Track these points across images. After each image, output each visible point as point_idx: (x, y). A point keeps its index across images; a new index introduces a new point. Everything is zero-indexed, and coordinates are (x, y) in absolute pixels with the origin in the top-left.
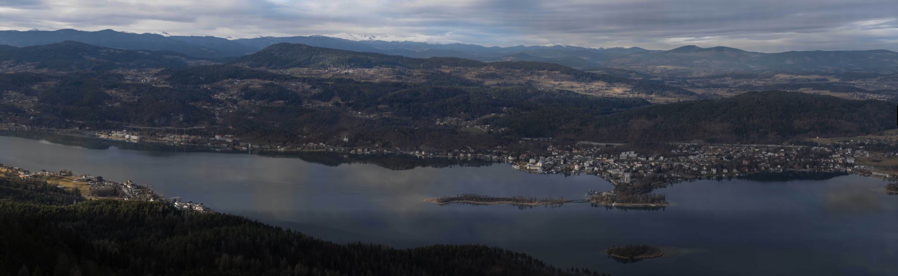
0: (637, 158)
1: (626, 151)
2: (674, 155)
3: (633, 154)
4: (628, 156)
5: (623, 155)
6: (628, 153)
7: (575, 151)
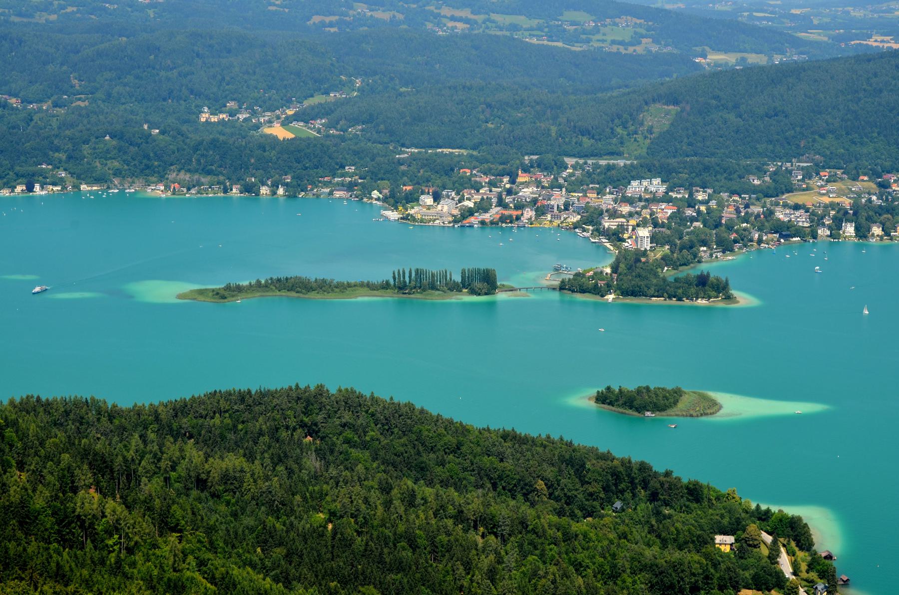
0: (667, 193)
1: (640, 178)
2: (754, 190)
3: (657, 186)
4: (646, 189)
5: (635, 188)
6: (645, 183)
7: (522, 178)
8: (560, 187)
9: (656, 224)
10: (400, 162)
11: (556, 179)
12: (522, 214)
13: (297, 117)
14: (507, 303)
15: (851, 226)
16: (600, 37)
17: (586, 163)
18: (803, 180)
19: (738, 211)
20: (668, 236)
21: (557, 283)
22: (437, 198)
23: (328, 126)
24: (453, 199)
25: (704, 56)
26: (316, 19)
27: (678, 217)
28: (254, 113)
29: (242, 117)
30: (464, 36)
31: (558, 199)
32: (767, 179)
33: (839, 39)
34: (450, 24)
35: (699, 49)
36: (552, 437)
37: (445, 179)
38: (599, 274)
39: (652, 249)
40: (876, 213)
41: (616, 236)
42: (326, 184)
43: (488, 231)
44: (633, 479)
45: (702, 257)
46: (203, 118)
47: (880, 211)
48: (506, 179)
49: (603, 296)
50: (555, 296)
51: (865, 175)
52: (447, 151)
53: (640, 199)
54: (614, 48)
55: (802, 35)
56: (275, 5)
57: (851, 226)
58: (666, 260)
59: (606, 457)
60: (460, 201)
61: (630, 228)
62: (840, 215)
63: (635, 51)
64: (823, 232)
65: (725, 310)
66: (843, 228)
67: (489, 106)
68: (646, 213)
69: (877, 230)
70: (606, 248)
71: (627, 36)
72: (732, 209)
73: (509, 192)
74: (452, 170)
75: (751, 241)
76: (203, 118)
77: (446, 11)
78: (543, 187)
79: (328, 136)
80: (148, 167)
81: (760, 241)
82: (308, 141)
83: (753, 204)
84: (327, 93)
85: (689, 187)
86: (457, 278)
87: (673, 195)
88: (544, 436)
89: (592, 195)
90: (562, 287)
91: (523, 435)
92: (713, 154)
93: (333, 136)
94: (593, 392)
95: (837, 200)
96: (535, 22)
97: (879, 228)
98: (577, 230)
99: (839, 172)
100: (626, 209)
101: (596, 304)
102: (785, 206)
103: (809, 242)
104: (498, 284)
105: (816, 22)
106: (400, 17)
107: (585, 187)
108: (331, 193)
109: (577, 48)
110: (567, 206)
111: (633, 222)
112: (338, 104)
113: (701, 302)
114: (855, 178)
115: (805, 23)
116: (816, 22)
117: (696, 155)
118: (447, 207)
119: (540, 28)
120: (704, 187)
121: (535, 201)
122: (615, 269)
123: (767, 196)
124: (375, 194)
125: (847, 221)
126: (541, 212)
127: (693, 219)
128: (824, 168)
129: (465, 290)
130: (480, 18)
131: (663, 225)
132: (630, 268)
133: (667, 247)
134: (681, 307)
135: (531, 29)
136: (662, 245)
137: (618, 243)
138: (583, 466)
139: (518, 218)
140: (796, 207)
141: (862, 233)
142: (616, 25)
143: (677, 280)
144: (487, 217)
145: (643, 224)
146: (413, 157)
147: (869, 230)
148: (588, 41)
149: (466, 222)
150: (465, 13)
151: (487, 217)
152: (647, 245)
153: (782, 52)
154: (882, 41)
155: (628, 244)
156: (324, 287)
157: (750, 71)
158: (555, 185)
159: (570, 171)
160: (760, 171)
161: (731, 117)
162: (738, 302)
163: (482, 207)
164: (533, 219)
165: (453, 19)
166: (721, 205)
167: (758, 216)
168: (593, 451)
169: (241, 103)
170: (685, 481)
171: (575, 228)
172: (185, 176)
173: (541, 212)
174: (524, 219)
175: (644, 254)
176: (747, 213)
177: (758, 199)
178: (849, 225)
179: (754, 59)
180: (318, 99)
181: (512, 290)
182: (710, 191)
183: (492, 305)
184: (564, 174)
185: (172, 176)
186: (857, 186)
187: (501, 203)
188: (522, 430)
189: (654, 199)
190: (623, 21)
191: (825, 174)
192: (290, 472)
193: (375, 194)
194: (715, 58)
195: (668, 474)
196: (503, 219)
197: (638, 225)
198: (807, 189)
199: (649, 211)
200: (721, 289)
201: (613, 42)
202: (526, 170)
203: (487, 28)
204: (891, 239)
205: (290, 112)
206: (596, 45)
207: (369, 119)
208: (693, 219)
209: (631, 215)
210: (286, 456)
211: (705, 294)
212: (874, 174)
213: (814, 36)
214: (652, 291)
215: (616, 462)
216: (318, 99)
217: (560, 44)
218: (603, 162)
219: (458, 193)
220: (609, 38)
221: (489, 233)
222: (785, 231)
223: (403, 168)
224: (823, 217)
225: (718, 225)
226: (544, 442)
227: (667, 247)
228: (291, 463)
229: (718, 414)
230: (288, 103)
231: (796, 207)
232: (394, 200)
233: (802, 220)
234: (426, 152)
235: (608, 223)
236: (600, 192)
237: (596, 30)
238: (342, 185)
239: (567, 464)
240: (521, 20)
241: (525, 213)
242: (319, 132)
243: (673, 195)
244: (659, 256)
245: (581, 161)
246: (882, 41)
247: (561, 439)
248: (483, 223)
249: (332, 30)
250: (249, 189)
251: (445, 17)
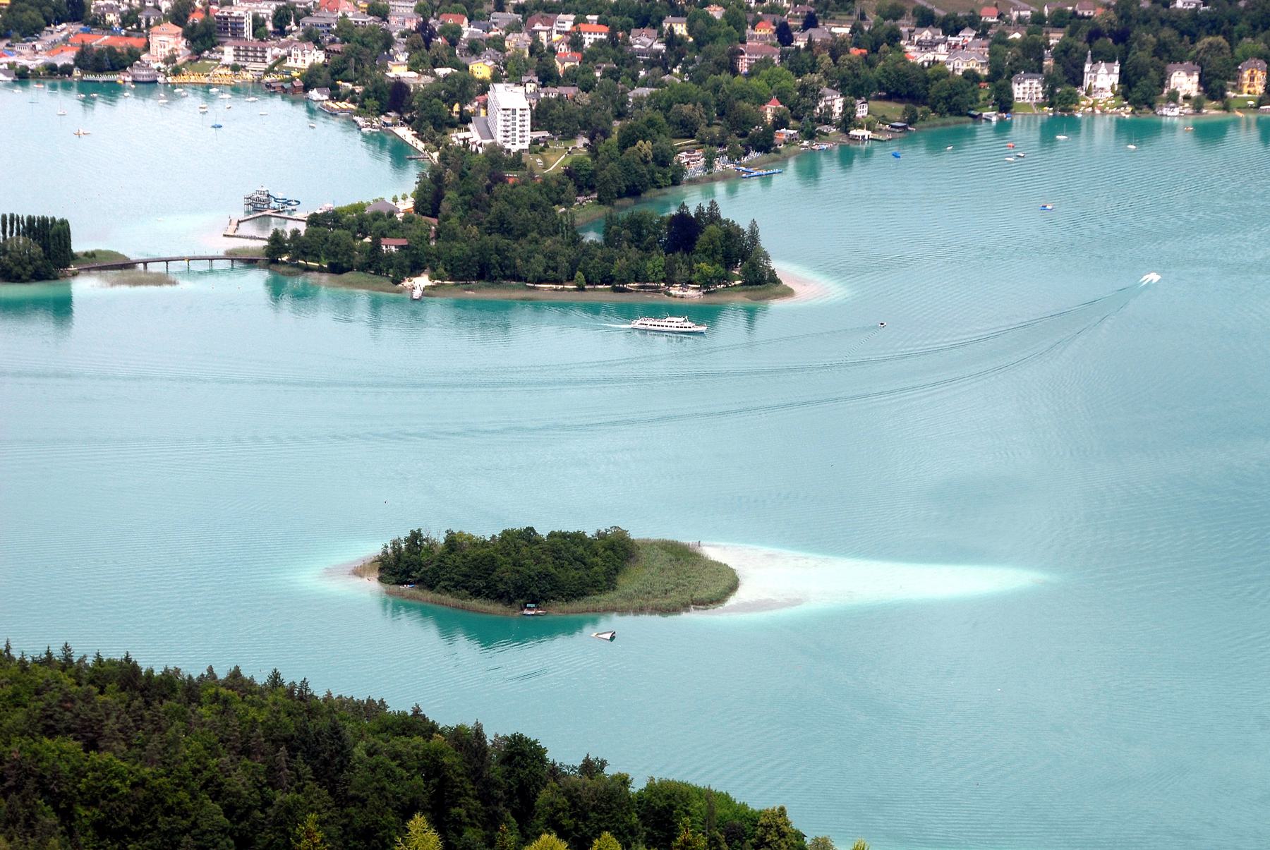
15: (1110, 72)
19: (784, 35)
20: (586, 110)
21: (258, 244)
36: (246, 674)
40: (1182, 33)
43: (39, 93)
44: (490, 784)
45: (681, 170)
57: (1110, 72)
58: (580, 179)
59: (415, 724)
64: (1026, 90)
66: (1087, 81)
69: (1184, 82)
72: (766, 31)
81: (848, 121)
88: (222, 674)
91: (158, 672)
94: (374, 548)
97: (1189, 74)
98: (314, 94)
103: (989, 121)
104: (78, 247)
125: (1098, 57)
133: (581, 141)
136: (570, 136)
138: (343, 752)
139: (132, 57)
147: (1163, 80)
162: (788, 293)
164: (180, 60)
168: (372, 709)
170: (638, 785)
171: (306, 88)
174: (153, 59)
175: (517, 162)
178: (1103, 68)
188: (152, 661)
195: (590, 768)
199: (526, 36)
204: (1226, 108)
211: (692, 271)
215: (437, 740)
226: (223, 690)
227: (581, 141)
229: (732, 601)
239: (293, 751)
241: (155, 41)
247: (275, 679)
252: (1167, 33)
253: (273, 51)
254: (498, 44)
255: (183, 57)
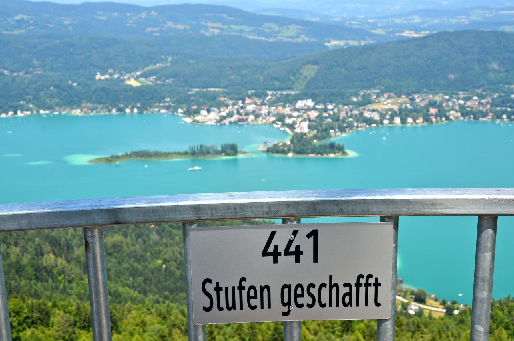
0: (314, 106)
1: (302, 99)
2: (354, 103)
3: (310, 103)
4: (305, 105)
5: (300, 104)
6: (304, 101)
7: (248, 101)
8: (265, 105)
9: (310, 120)
10: (191, 95)
11: (263, 101)
12: (248, 118)
13: (142, 76)
14: (242, 159)
16: (281, 34)
17: (277, 93)
18: (376, 98)
19: (347, 113)
21: (265, 149)
22: (209, 111)
23: (157, 79)
24: (216, 112)
25: (329, 42)
26: (149, 29)
27: (320, 117)
28: (121, 75)
29: (116, 76)
30: (219, 36)
31: (265, 110)
32: (360, 98)
33: (390, 33)
34: (212, 30)
35: (327, 39)
37: (212, 102)
38: (284, 145)
39: (309, 132)
41: (292, 127)
42: (157, 107)
46: (98, 77)
47: (411, 111)
48: (240, 102)
49: (287, 154)
50: (265, 155)
51: (404, 94)
52: (212, 89)
53: (302, 109)
54: (288, 40)
55: (374, 31)
56: (128, 23)
58: (315, 137)
60: (220, 112)
61: (298, 123)
62: (393, 114)
63: (298, 41)
64: (386, 122)
65: (343, 159)
67: (231, 68)
68: (305, 116)
69: (410, 120)
70: (287, 133)
71: (294, 34)
72: (344, 113)
73: (242, 108)
74: (215, 98)
75: (353, 126)
76: (98, 77)
77: (210, 24)
78: (258, 105)
79: (157, 84)
80: (72, 101)
81: (357, 127)
82: (148, 87)
83: (354, 110)
84: (155, 64)
85: (325, 103)
86: (219, 148)
87: (317, 107)
89: (280, 108)
90: (268, 151)
92: (335, 88)
93: (159, 84)
95: (392, 107)
96: (251, 29)
99: (392, 94)
100: (296, 114)
101: (284, 159)
102: (369, 110)
104: (239, 150)
105: (379, 25)
106: (188, 27)
107: (276, 104)
108: (159, 111)
109: (271, 40)
110: (269, 113)
111: (299, 120)
112: (161, 69)
113: (332, 156)
114: (399, 96)
115: (375, 26)
116: (379, 25)
117: (327, 88)
118: (214, 116)
119: (253, 31)
120: (331, 102)
121: (254, 112)
122: (292, 141)
123: (360, 106)
124: (180, 110)
126: (257, 116)
127: (326, 118)
128: (385, 92)
129: (223, 154)
130: (226, 27)
131: (313, 121)
132: (299, 141)
134: (323, 159)
135: (249, 32)
136: (313, 130)
137: (293, 130)
139: (247, 120)
140: (373, 111)
141: (404, 121)
142: (288, 29)
143: (320, 146)
144: (232, 119)
145: (304, 120)
146: (197, 93)
147: (406, 120)
148: (276, 37)
149: (223, 122)
150: (219, 25)
151: (232, 119)
152: (306, 130)
153: (364, 39)
154: (410, 34)
155: (297, 130)
156: (157, 155)
157: (350, 49)
158: (263, 104)
159: (269, 97)
160: (356, 95)
161: (343, 70)
163: (230, 115)
165: (213, 28)
166: (339, 111)
167: (356, 115)
169: (115, 70)
172: (90, 105)
173: (257, 116)
175: (305, 134)
176: (351, 114)
177: (356, 107)
179: (352, 43)
180: (151, 67)
181: (244, 153)
182: (334, 104)
183: (236, 161)
184: (267, 99)
185: (84, 105)
186: (400, 100)
187: (238, 113)
189: (309, 109)
190: (291, 27)
191: (386, 95)
192: (145, 242)
193: (180, 110)
194: (334, 43)
196: (240, 120)
197: (302, 121)
198: (379, 102)
200: (340, 149)
201: (288, 37)
202: (249, 97)
203: (229, 32)
205: (138, 73)
206: (280, 38)
207: (175, 75)
208: (326, 118)
209: (298, 117)
210: (142, 234)
212: (408, 95)
213: (378, 32)
214: (309, 151)
216: (151, 67)
217: (263, 38)
218: (285, 93)
219: (218, 109)
220: (286, 35)
221: (233, 127)
222: (369, 121)
223: (192, 98)
224: (385, 115)
225: (338, 120)
228: (145, 238)
230: (137, 69)
231: (373, 111)
232: (189, 113)
233: (376, 117)
234: (203, 91)
235: (288, 121)
236: (284, 106)
237: (279, 32)
238: (164, 107)
240: (245, 28)
242: (152, 82)
243: (317, 107)
244: (312, 135)
245: (275, 92)
246: (410, 34)
248: (230, 123)
249: (157, 34)
250: (120, 110)
251: (209, 27)
252: (407, 112)
253: (268, 118)
254: (302, 116)
255: (254, 120)
